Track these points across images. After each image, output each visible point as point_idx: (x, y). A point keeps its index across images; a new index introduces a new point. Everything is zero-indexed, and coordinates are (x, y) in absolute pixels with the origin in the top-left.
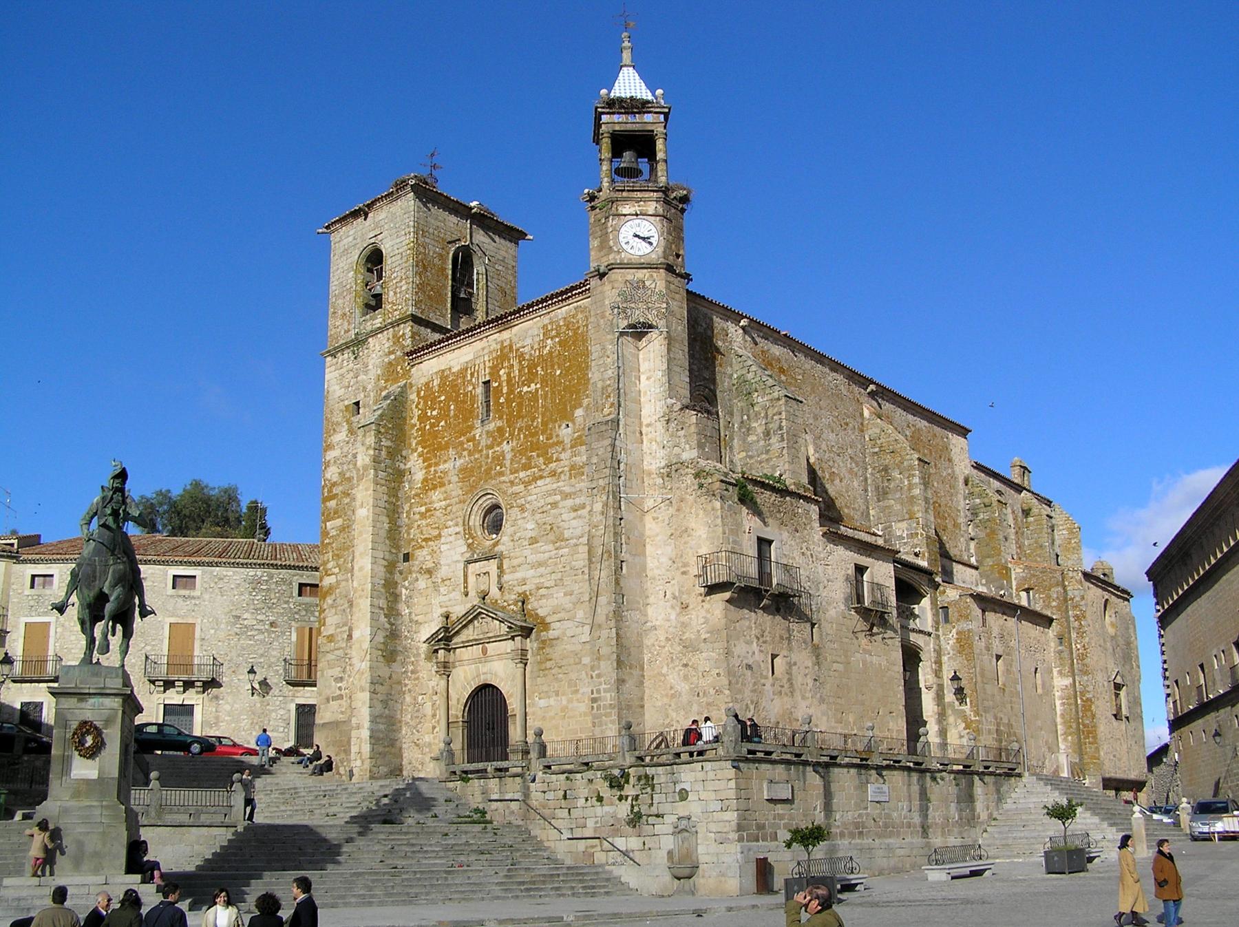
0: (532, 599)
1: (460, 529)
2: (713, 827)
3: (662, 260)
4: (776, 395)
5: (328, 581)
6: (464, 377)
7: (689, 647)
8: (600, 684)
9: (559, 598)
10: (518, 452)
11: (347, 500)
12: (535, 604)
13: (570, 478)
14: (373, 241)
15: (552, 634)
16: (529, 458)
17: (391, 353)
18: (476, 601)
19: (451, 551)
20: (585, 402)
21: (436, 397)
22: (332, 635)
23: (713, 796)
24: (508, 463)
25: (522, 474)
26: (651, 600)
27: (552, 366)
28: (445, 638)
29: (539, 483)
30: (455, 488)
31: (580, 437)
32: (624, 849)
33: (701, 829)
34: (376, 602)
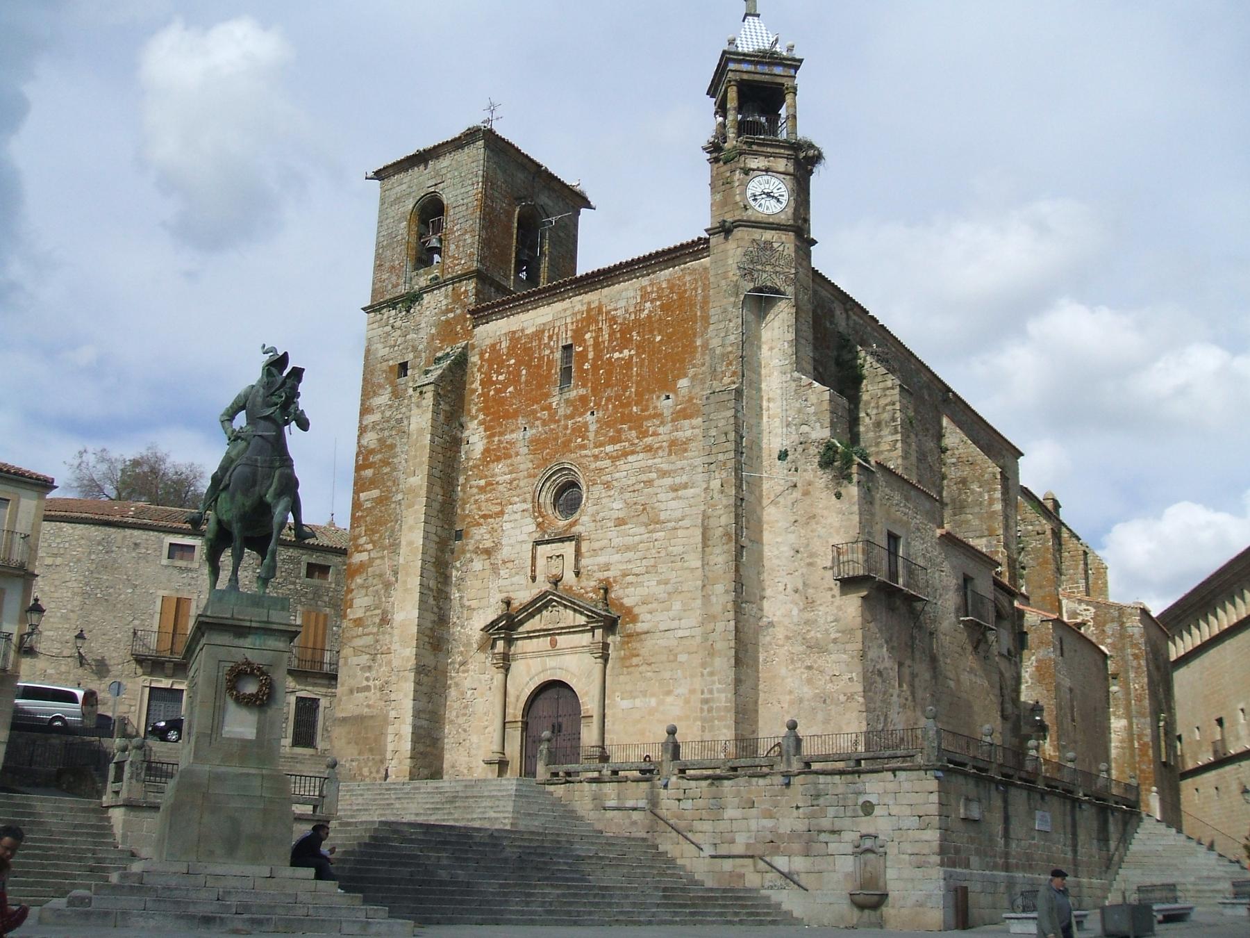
0: (616, 587)
1: (530, 506)
2: (909, 848)
3: (791, 222)
4: (889, 384)
5: (358, 558)
6: (540, 340)
7: (815, 647)
8: (714, 682)
9: (651, 586)
10: (604, 424)
11: (386, 470)
12: (620, 593)
13: (670, 454)
14: (432, 189)
15: (640, 627)
16: (619, 431)
17: (448, 311)
18: (547, 587)
19: (517, 530)
20: (691, 372)
21: (503, 361)
22: (360, 619)
23: (908, 811)
24: (591, 435)
25: (609, 448)
26: (768, 593)
27: (651, 332)
28: (507, 627)
29: (630, 458)
30: (524, 461)
31: (684, 409)
32: (786, 870)
33: (892, 850)
34: (425, 583)
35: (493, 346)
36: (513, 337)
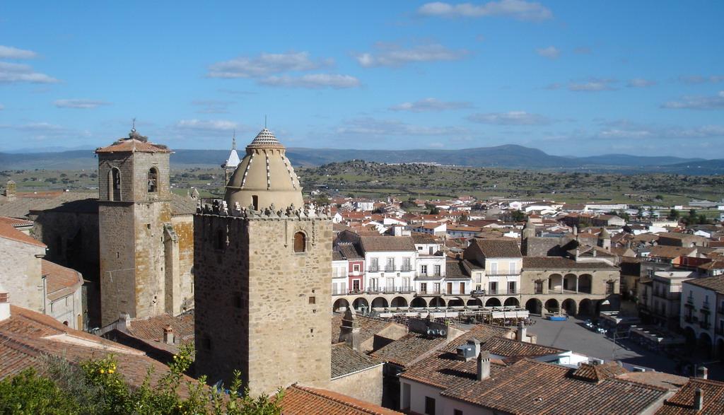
11: (146, 259)
35: (177, 226)
36: (183, 224)
